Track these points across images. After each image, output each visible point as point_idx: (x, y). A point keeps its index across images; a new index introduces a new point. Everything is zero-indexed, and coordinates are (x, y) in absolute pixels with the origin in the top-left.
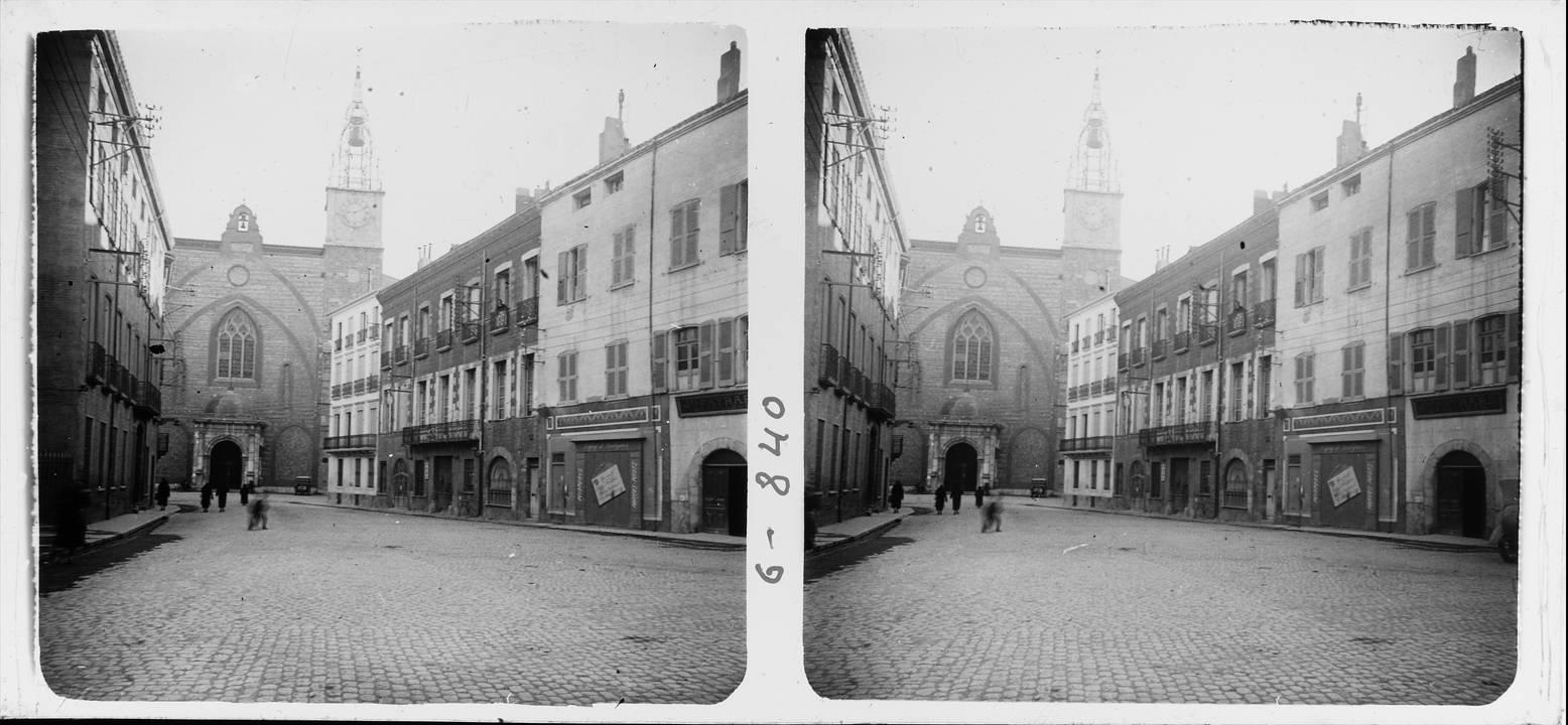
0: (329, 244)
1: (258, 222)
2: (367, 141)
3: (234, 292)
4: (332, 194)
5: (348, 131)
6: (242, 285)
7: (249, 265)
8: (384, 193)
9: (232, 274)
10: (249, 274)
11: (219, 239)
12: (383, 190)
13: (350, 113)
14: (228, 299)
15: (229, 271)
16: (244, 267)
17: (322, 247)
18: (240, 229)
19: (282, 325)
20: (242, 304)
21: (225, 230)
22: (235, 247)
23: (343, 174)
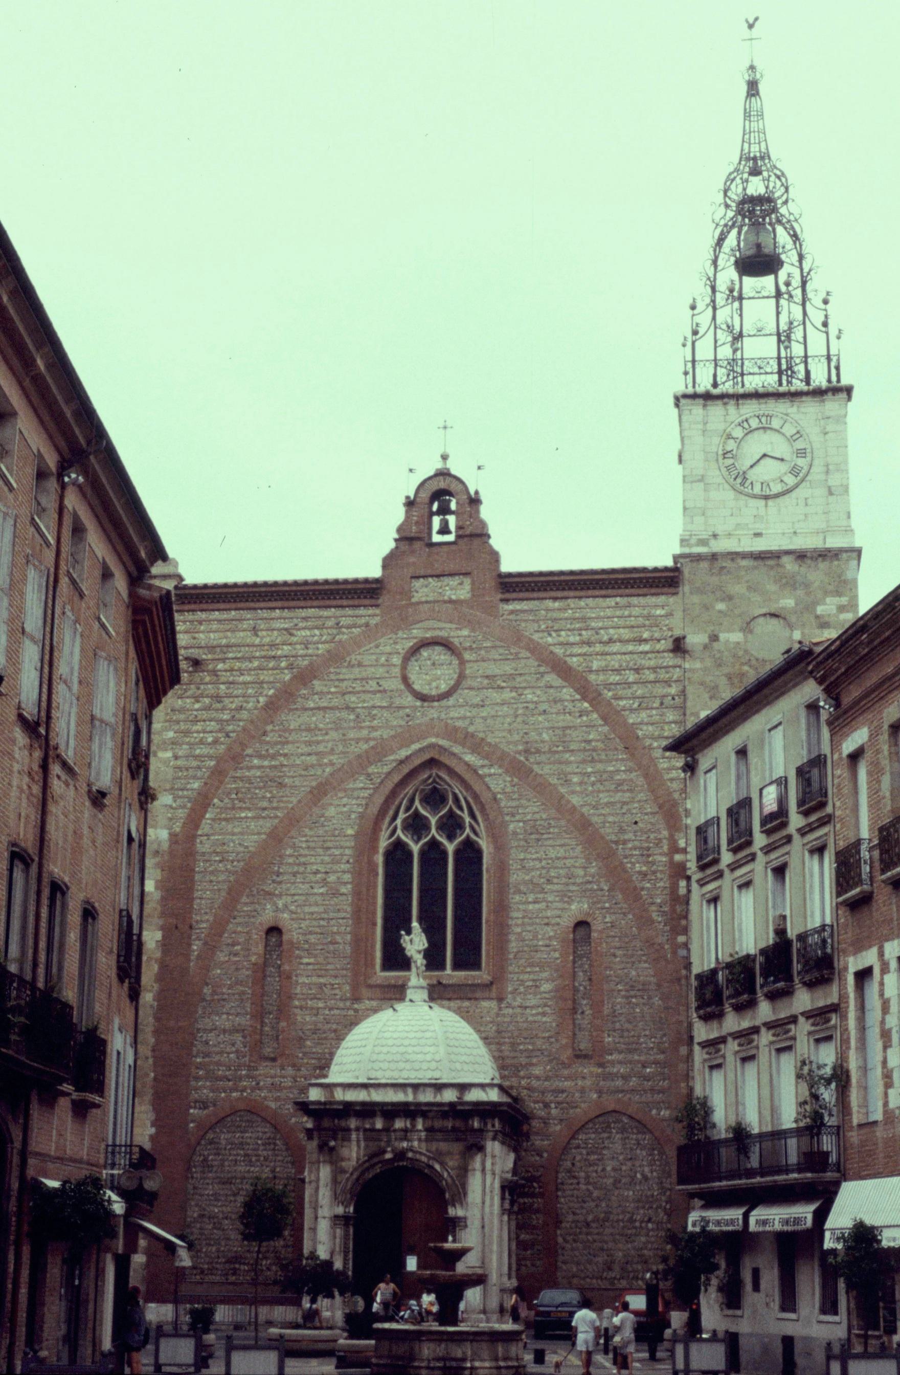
0: (687, 550)
1: (485, 512)
2: (789, 257)
3: (420, 719)
4: (696, 410)
5: (731, 240)
6: (447, 695)
7: (460, 635)
8: (849, 390)
10: (462, 662)
11: (374, 571)
12: (844, 382)
13: (736, 192)
14: (404, 739)
15: (406, 659)
16: (446, 644)
17: (670, 563)
18: (437, 538)
19: (561, 806)
20: (442, 749)
21: (393, 545)
22: (424, 590)
23: (725, 352)
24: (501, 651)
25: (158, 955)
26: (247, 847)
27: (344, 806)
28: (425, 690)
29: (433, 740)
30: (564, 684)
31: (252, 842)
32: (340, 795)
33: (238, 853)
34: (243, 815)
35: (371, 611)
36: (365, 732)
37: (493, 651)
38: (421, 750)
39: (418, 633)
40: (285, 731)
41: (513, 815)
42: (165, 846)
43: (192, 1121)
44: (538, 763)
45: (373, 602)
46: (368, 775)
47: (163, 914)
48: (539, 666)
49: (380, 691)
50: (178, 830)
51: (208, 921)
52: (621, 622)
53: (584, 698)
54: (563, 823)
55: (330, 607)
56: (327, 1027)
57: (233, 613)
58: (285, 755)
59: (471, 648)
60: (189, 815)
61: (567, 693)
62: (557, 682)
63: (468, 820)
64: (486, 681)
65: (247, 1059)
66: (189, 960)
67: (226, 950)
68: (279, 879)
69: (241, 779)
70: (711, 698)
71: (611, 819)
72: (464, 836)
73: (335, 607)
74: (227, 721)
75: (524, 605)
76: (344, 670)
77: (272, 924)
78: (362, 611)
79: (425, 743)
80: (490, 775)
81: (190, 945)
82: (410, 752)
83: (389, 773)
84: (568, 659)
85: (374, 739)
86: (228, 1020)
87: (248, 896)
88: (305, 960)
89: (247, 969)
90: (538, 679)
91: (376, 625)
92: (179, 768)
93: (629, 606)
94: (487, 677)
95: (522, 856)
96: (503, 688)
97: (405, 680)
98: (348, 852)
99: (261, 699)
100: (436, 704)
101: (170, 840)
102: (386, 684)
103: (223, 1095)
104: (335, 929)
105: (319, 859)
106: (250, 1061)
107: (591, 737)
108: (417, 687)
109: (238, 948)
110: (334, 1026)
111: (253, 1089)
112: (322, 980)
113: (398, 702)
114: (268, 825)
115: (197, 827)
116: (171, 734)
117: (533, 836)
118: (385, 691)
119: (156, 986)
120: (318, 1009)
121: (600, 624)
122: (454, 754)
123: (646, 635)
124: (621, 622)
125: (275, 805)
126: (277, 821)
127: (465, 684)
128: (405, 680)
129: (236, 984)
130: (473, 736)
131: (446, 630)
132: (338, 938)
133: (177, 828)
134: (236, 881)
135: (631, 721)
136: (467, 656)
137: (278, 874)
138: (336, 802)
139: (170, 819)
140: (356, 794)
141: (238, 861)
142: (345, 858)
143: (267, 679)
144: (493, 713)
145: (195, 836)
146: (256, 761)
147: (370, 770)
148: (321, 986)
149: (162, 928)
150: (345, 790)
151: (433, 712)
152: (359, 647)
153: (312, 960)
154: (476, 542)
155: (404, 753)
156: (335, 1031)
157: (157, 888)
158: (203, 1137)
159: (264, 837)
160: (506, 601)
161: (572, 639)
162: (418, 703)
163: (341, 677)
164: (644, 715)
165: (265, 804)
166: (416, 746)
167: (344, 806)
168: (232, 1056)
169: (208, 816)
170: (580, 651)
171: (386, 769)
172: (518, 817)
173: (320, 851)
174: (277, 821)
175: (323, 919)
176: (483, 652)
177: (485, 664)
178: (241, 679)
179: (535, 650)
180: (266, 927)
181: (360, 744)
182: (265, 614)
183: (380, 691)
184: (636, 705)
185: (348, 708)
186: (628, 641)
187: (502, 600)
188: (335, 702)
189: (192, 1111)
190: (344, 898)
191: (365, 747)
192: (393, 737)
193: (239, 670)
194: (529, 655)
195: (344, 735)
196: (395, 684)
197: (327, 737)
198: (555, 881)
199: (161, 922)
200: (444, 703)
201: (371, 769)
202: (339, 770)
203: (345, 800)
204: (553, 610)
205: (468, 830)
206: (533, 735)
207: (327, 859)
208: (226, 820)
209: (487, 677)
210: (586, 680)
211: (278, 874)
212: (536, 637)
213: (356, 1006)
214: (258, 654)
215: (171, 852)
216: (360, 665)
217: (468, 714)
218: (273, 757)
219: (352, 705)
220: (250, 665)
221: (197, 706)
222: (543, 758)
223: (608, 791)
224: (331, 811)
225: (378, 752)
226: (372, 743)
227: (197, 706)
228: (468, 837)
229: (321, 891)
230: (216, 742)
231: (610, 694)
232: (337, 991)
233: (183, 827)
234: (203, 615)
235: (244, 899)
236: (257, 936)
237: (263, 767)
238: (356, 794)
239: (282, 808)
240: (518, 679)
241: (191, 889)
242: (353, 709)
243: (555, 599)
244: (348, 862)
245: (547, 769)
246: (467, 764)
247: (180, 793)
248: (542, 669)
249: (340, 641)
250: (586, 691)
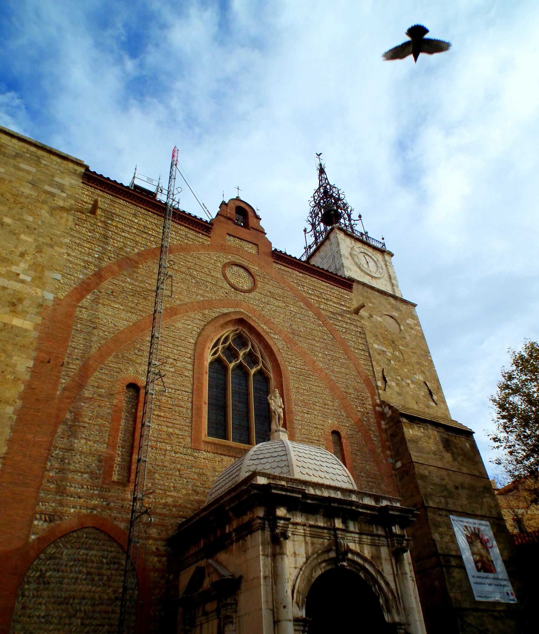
7: (254, 268)
9: (229, 273)
24: (275, 283)
25: (27, 377)
26: (116, 326)
27: (188, 325)
28: (237, 285)
29: (242, 310)
30: (309, 309)
31: (122, 325)
32: (185, 318)
33: (109, 328)
34: (117, 306)
35: (205, 237)
36: (201, 292)
37: (271, 281)
38: (236, 312)
39: (231, 258)
40: (150, 271)
41: (289, 363)
42: (50, 304)
43: (34, 534)
44: (300, 341)
45: (207, 234)
46: (204, 314)
47: (38, 349)
48: (295, 297)
49: (211, 275)
50: (62, 297)
51: (78, 365)
52: (331, 294)
53: (319, 319)
54: (316, 374)
55: (183, 225)
56: (173, 466)
57: (122, 201)
58: (149, 284)
59: (260, 276)
60: (72, 292)
61: (310, 313)
62: (305, 307)
63: (261, 359)
64: (269, 294)
65: (100, 480)
66: (57, 390)
67: (91, 389)
68: (140, 353)
69: (116, 285)
70: (376, 340)
71: (341, 380)
72: (259, 367)
73: (185, 226)
74: (110, 250)
75: (286, 269)
76: (188, 257)
77: (131, 381)
78: (200, 235)
79: (238, 310)
80: (275, 338)
81: (59, 378)
82: (227, 311)
83: (217, 317)
84: (310, 300)
85: (207, 297)
86: (86, 443)
87: (114, 358)
88: (156, 413)
89: (109, 408)
90: (295, 303)
91: (208, 245)
92: (71, 262)
93: (332, 289)
94: (270, 292)
95: (297, 386)
96: (278, 300)
97: (225, 276)
98: (189, 351)
99: (136, 250)
100: (243, 294)
101: (54, 301)
102: (213, 273)
103: (72, 510)
104: (180, 397)
105: (169, 350)
106: (103, 483)
107: (326, 338)
108: (232, 281)
109: (103, 391)
110: (179, 466)
111: (103, 508)
112: (171, 430)
113: (220, 284)
114: (134, 318)
115: (79, 300)
116: (67, 241)
117: (302, 377)
118: (213, 276)
119: (19, 403)
120: (166, 450)
121: (322, 291)
122: (254, 320)
123: (343, 303)
124: (331, 294)
125: (141, 308)
126: (141, 318)
127: (257, 290)
128: (225, 276)
129: (97, 417)
130: (264, 316)
131: (245, 264)
132: (182, 404)
133: (62, 295)
134: (106, 344)
135: (343, 337)
136: (258, 278)
137: (139, 350)
138: (183, 321)
139: (57, 289)
140: (195, 321)
141: (109, 332)
142: (189, 355)
143: (140, 241)
144: (273, 309)
145: (75, 306)
146: (129, 280)
147: (204, 311)
148: (170, 435)
149: (36, 359)
150: (189, 317)
151: (241, 296)
152: (199, 251)
153: (162, 414)
154: (261, 234)
155: (226, 311)
156: (179, 470)
157: (35, 329)
158: (43, 551)
159: (131, 324)
160: (277, 263)
161: (310, 292)
162: (233, 290)
163: (187, 259)
164: (349, 336)
165: (133, 305)
166: (231, 310)
167: (188, 325)
168: (85, 475)
169: (88, 297)
170: (314, 298)
171: (214, 315)
172: (292, 364)
173: (171, 346)
174: (141, 318)
175: (172, 388)
176: (266, 280)
177: (268, 286)
178: (123, 234)
179: (292, 289)
180: (127, 383)
181: (199, 297)
182: (143, 211)
183: (211, 275)
184: (344, 331)
185: (190, 275)
186: (335, 303)
187: (274, 262)
188: (183, 269)
189: (36, 522)
190: (187, 379)
191: (202, 299)
192: (220, 300)
193: (122, 229)
194: (289, 289)
195: (188, 288)
196: (220, 276)
197: (178, 285)
198: (317, 404)
199: (34, 354)
200: (247, 294)
201: (206, 312)
202: (185, 304)
203: (189, 322)
204: (300, 277)
205: (261, 365)
206: (295, 327)
207: (176, 351)
208: (104, 305)
209: (270, 292)
210: (319, 311)
211: (139, 350)
212: (291, 283)
213: (196, 454)
214: (136, 227)
215: (55, 310)
216: (198, 258)
217: (262, 306)
218: (141, 282)
219: (194, 275)
220: (130, 230)
221: (89, 234)
222: (302, 339)
223: (338, 366)
224: (179, 325)
225: (209, 304)
226: (205, 299)
227: (89, 234)
228: (261, 368)
229: (171, 370)
230: (98, 258)
231: (331, 322)
232: (182, 440)
233: (67, 296)
234: (102, 193)
235: (111, 358)
236: (120, 387)
237: (133, 284)
238: (195, 321)
239: (145, 312)
240: (286, 299)
241: (66, 339)
242: (194, 278)
243: (300, 272)
244: (190, 358)
245: (305, 345)
246: (263, 328)
247: (69, 276)
248: (297, 299)
249: (187, 243)
250: (319, 316)
